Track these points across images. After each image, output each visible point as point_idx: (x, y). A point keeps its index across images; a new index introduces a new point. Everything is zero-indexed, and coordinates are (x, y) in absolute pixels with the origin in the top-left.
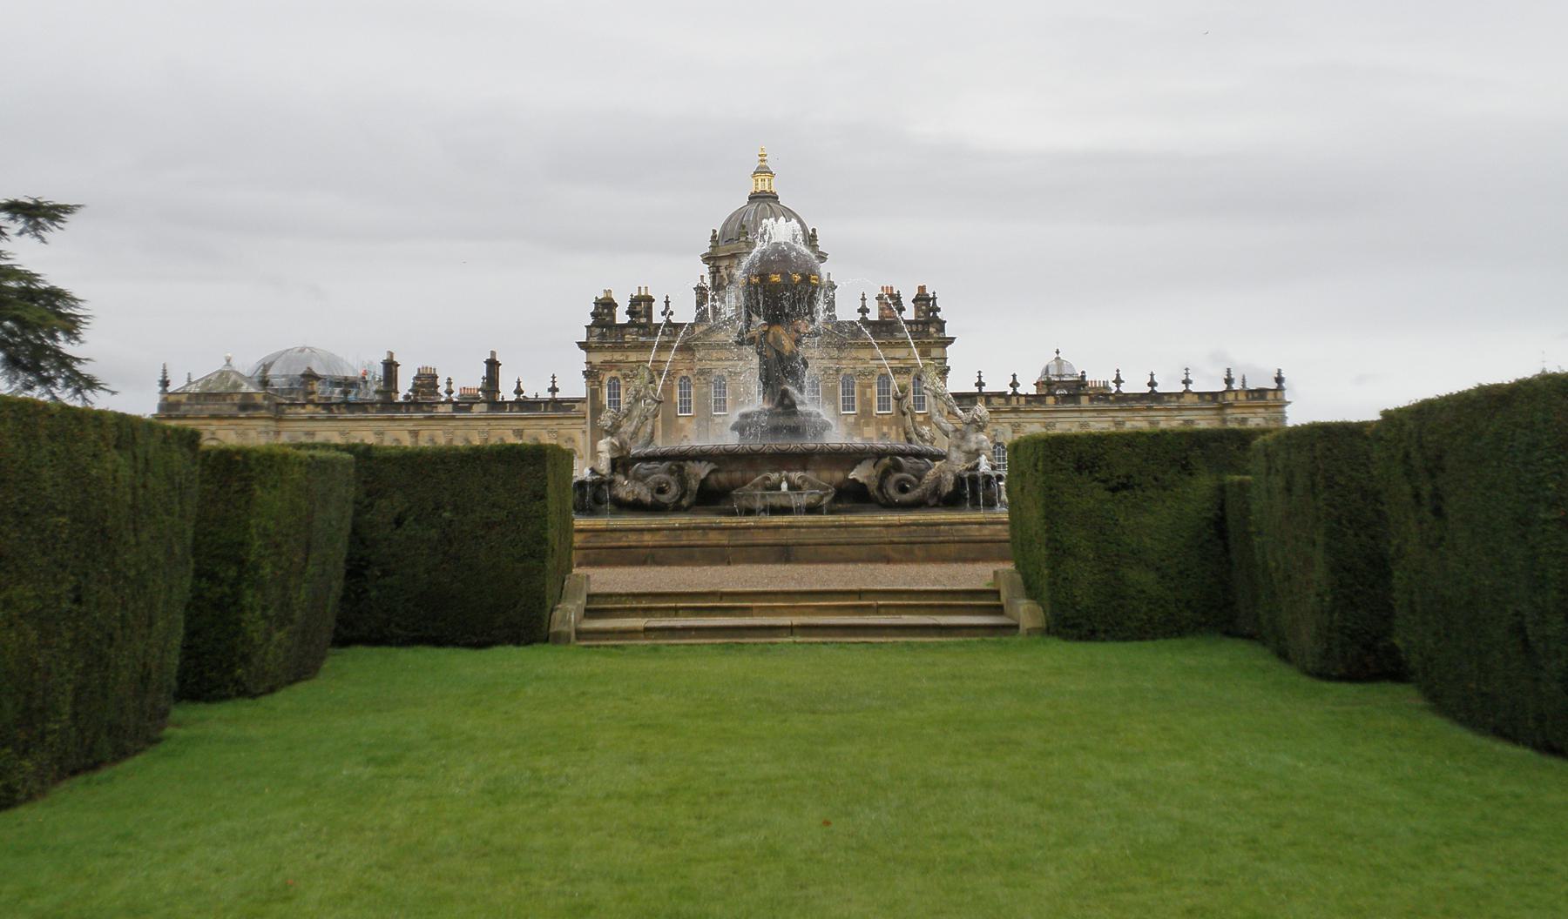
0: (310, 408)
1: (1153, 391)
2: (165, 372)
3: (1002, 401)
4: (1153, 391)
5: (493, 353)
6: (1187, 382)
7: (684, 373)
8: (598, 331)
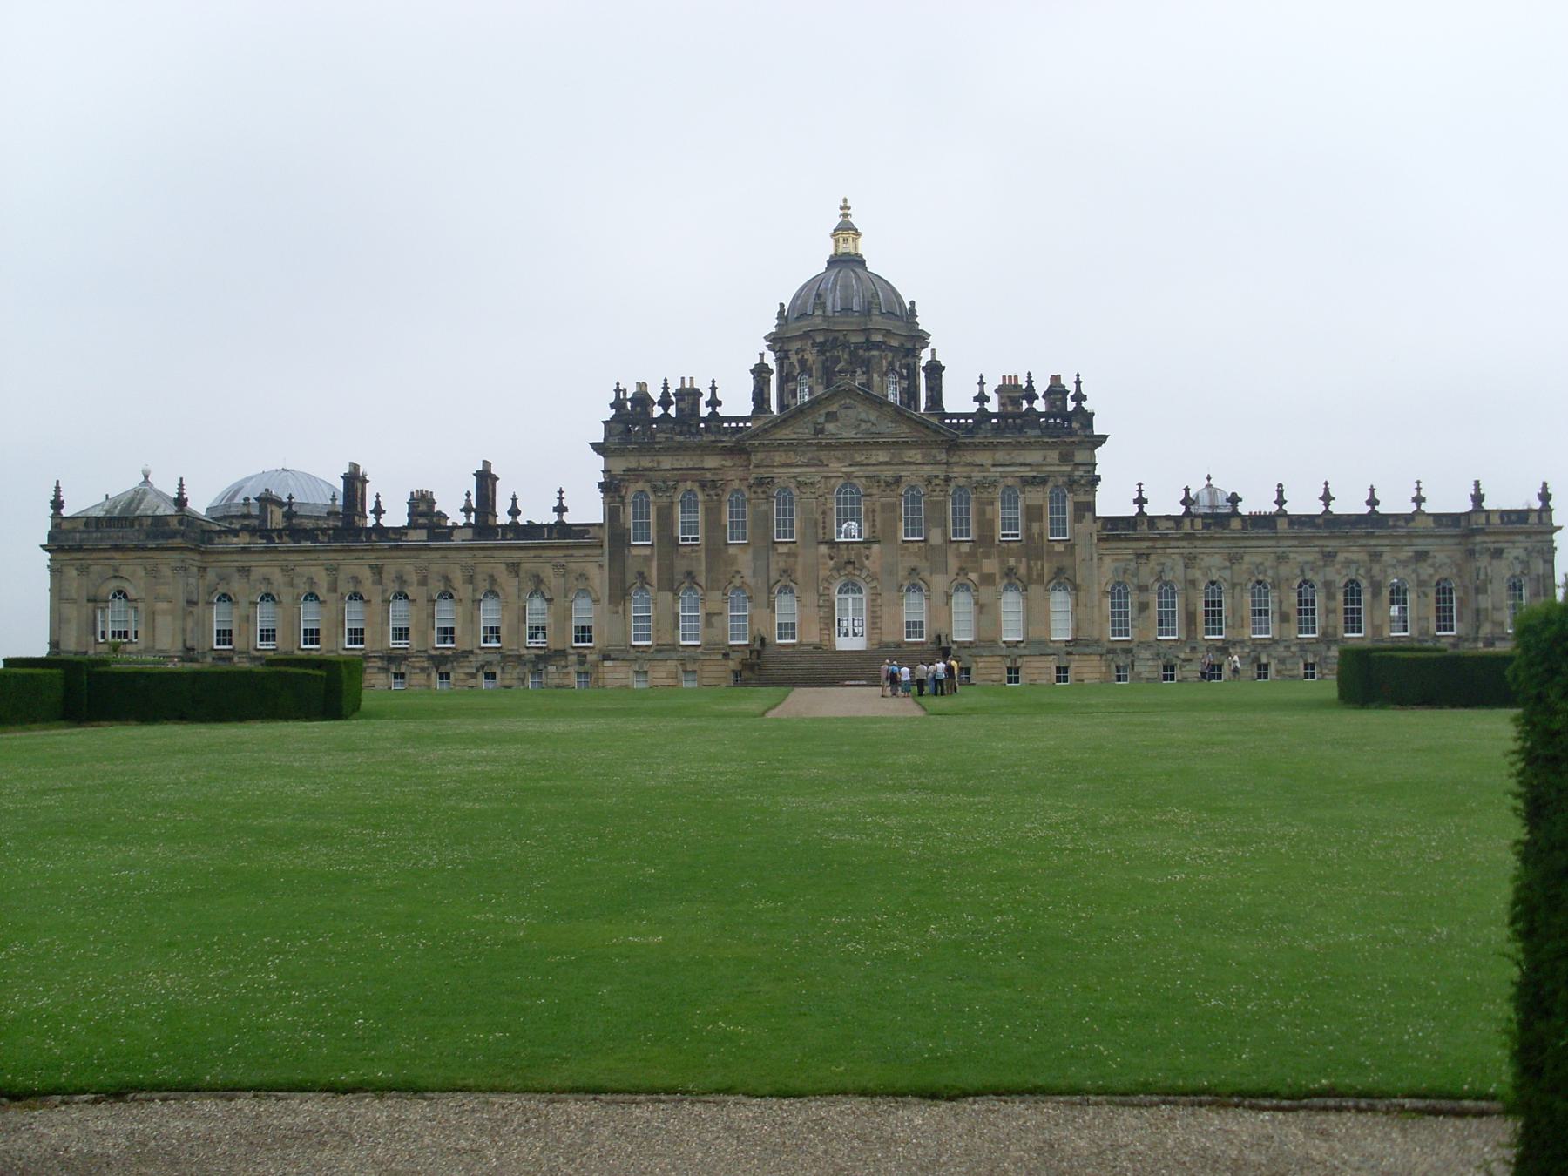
1: (1373, 511)
2: (58, 488)
3: (1171, 524)
4: (1373, 511)
6: (1419, 500)
7: (736, 484)
8: (620, 427)
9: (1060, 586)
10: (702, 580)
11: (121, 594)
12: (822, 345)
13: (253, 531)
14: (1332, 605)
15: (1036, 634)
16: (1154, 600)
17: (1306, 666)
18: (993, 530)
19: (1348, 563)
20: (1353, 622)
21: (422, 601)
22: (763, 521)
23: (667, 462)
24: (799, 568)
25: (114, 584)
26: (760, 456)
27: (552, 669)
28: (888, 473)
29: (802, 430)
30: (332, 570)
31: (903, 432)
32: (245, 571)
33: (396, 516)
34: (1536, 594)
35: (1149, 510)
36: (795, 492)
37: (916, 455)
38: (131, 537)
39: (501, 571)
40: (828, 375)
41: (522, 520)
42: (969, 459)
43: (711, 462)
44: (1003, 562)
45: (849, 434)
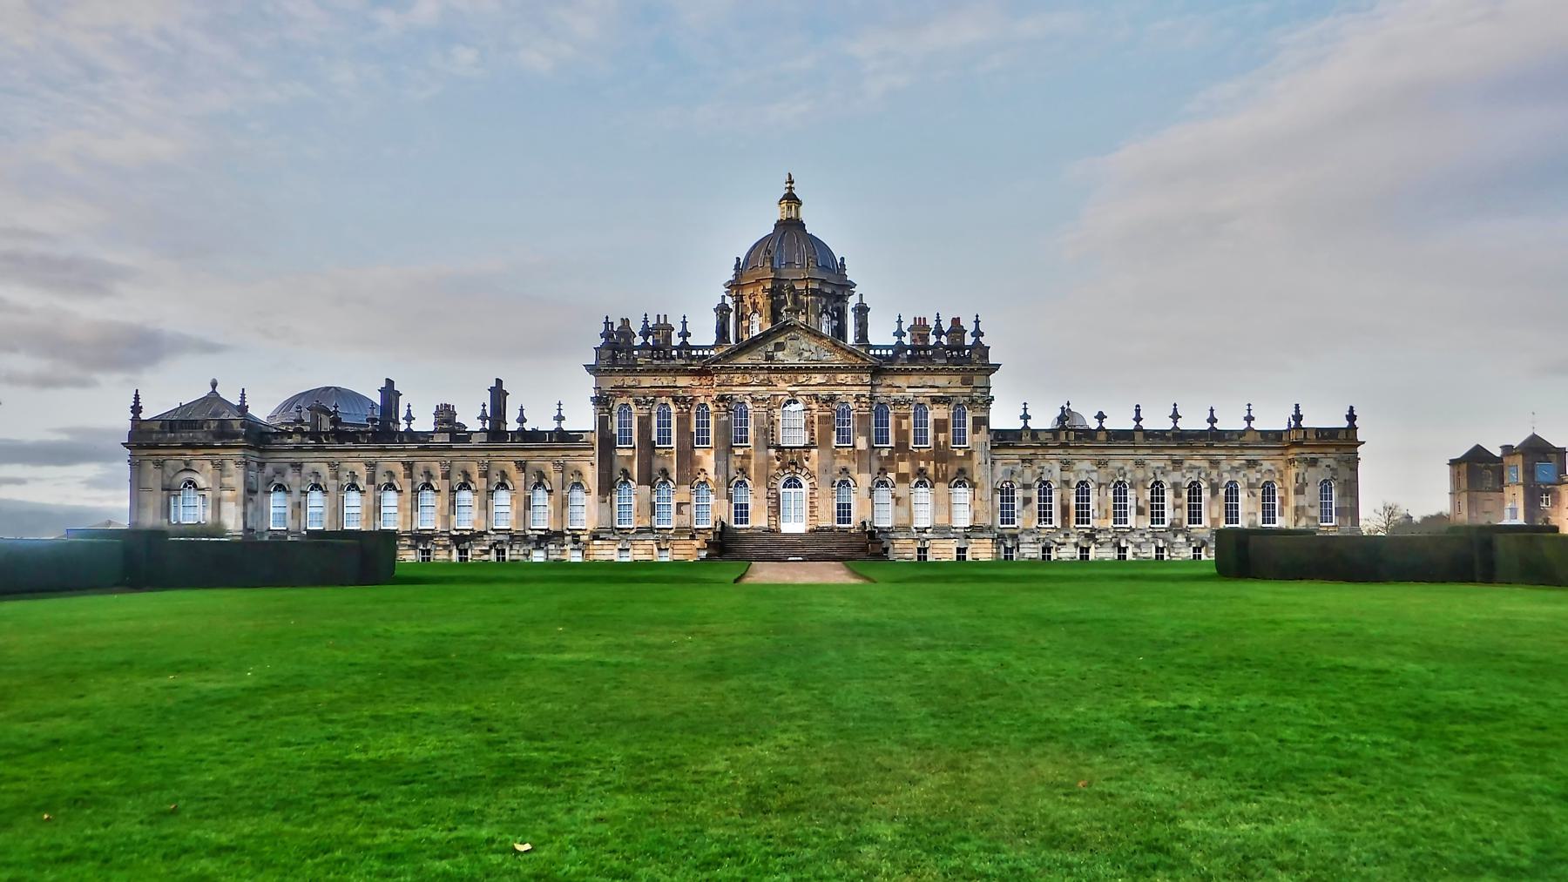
0: (297, 438)
1: (1213, 428)
3: (1050, 435)
4: (1213, 428)
5: (499, 382)
6: (1249, 419)
7: (702, 400)
9: (960, 483)
10: (674, 476)
11: (191, 484)
12: (771, 290)
13: (304, 434)
14: (1179, 501)
15: (942, 520)
16: (1035, 493)
17: (1157, 549)
18: (907, 438)
19: (1191, 468)
20: (1195, 517)
21: (445, 492)
22: (724, 429)
23: (647, 381)
24: (752, 467)
25: (187, 475)
26: (724, 377)
27: (551, 547)
28: (823, 392)
29: (757, 357)
30: (372, 466)
31: (837, 359)
32: (298, 466)
33: (424, 422)
34: (1342, 496)
35: (1032, 425)
36: (750, 406)
37: (849, 378)
38: (200, 436)
39: (511, 468)
40: (775, 315)
41: (528, 427)
42: (889, 382)
43: (683, 381)
44: (914, 464)
45: (793, 361)
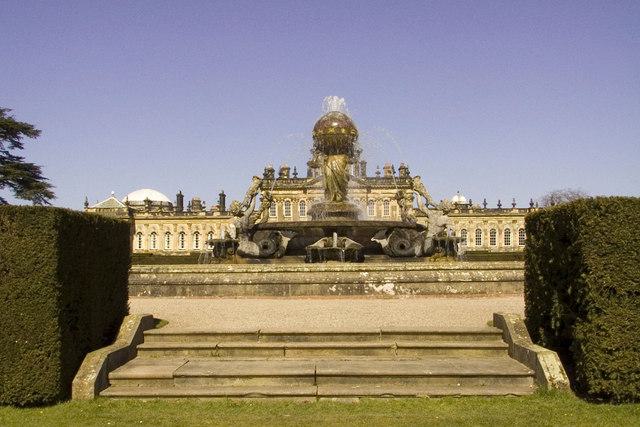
6: (514, 205)
19: (492, 224)
20: (493, 242)
43: (294, 192)
